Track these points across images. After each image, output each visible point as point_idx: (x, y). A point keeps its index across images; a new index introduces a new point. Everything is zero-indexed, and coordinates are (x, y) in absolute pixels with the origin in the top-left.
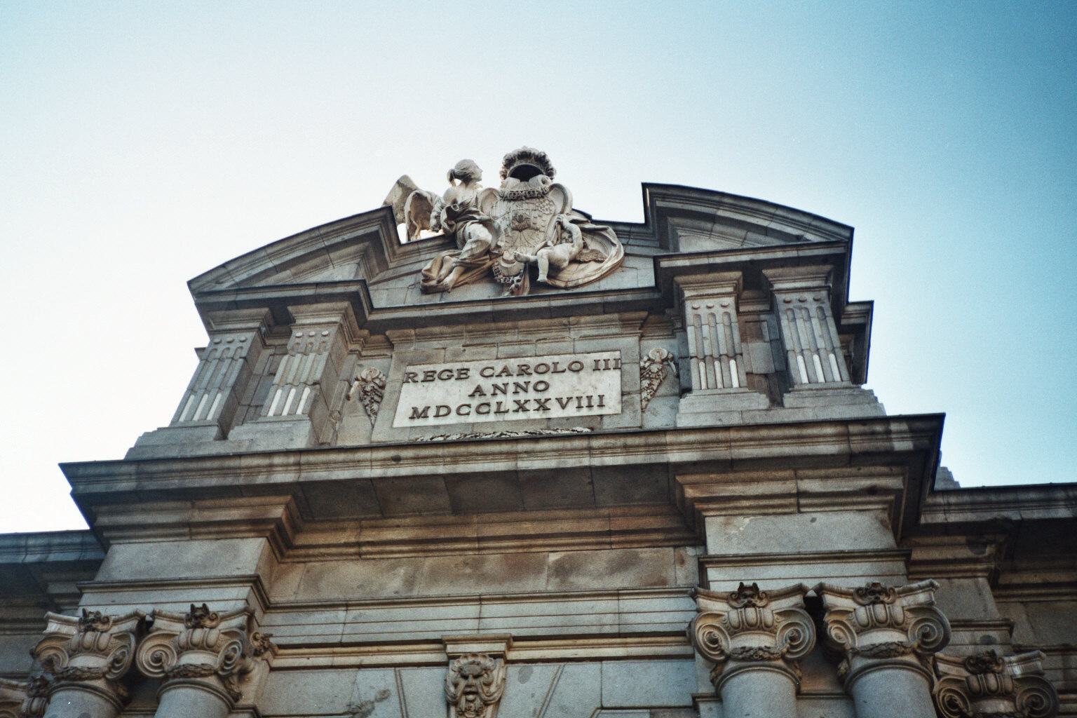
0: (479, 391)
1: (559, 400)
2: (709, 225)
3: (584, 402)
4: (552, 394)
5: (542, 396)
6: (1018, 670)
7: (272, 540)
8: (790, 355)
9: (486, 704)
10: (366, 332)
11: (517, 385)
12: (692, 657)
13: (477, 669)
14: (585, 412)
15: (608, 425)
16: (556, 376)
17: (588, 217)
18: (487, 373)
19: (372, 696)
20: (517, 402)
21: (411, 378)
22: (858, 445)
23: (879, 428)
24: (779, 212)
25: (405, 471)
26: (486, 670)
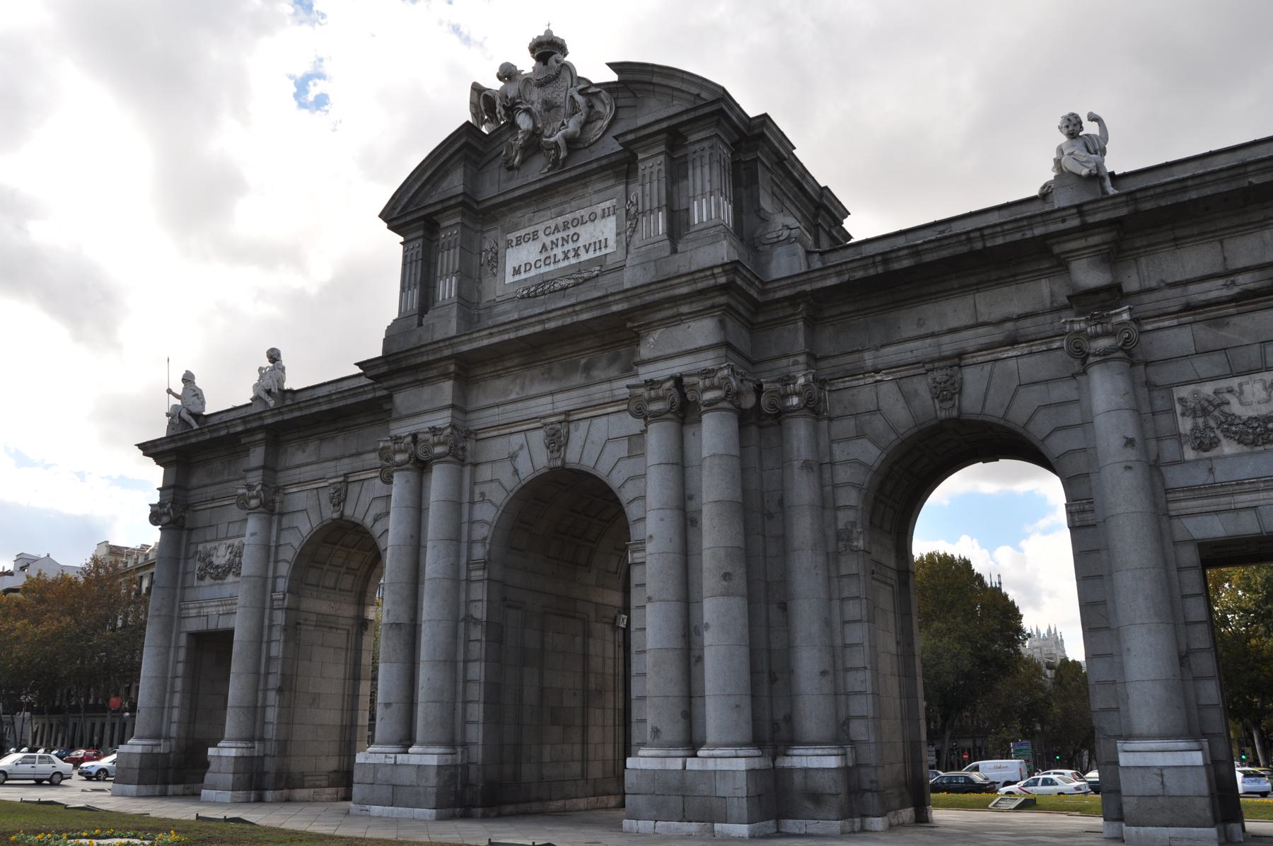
1: (585, 246)
2: (651, 88)
4: (581, 243)
5: (575, 246)
7: (455, 379)
9: (560, 447)
10: (480, 216)
11: (563, 239)
13: (553, 431)
14: (598, 254)
15: (609, 261)
16: (583, 226)
17: (589, 82)
18: (547, 233)
20: (564, 252)
21: (509, 244)
22: (700, 286)
23: (708, 273)
24: (685, 76)
25: (496, 339)
26: (558, 431)
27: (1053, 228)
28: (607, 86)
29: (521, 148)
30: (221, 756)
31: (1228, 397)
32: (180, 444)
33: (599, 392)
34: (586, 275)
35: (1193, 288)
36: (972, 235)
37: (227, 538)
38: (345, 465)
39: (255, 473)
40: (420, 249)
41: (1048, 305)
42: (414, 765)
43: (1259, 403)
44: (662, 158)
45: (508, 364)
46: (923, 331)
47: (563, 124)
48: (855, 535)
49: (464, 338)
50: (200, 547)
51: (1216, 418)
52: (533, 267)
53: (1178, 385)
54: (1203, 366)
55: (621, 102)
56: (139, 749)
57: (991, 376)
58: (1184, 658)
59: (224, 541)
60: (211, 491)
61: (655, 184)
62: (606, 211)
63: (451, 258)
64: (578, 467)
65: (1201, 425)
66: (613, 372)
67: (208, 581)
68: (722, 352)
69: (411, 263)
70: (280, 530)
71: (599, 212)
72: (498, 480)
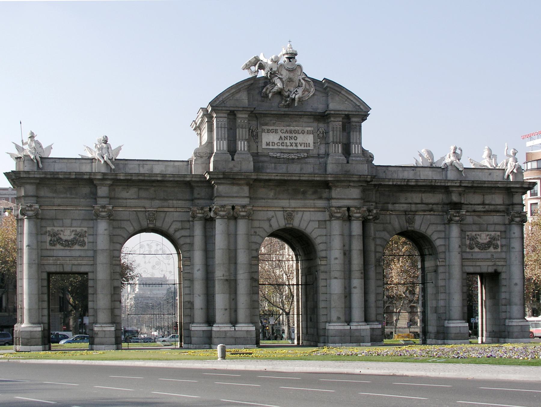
0: (281, 136)
1: (300, 143)
2: (339, 93)
4: (298, 141)
5: (296, 142)
8: (351, 144)
11: (290, 137)
12: (325, 211)
13: (290, 214)
14: (305, 148)
17: (307, 76)
18: (282, 131)
19: (271, 216)
20: (290, 143)
21: (263, 131)
22: (361, 179)
27: (453, 184)
30: (104, 331)
31: (478, 236)
33: (310, 202)
34: (303, 156)
36: (433, 181)
37: (71, 227)
38: (157, 203)
39: (104, 200)
40: (226, 123)
41: (441, 201)
42: (245, 331)
44: (341, 123)
45: (270, 184)
46: (407, 202)
47: (296, 91)
49: (265, 174)
51: (475, 242)
52: (276, 145)
53: (467, 231)
54: (474, 227)
55: (317, 88)
56: (39, 329)
59: (68, 228)
60: (57, 201)
63: (244, 132)
65: (472, 243)
66: (313, 197)
67: (59, 246)
68: (362, 201)
70: (113, 228)
71: (306, 131)
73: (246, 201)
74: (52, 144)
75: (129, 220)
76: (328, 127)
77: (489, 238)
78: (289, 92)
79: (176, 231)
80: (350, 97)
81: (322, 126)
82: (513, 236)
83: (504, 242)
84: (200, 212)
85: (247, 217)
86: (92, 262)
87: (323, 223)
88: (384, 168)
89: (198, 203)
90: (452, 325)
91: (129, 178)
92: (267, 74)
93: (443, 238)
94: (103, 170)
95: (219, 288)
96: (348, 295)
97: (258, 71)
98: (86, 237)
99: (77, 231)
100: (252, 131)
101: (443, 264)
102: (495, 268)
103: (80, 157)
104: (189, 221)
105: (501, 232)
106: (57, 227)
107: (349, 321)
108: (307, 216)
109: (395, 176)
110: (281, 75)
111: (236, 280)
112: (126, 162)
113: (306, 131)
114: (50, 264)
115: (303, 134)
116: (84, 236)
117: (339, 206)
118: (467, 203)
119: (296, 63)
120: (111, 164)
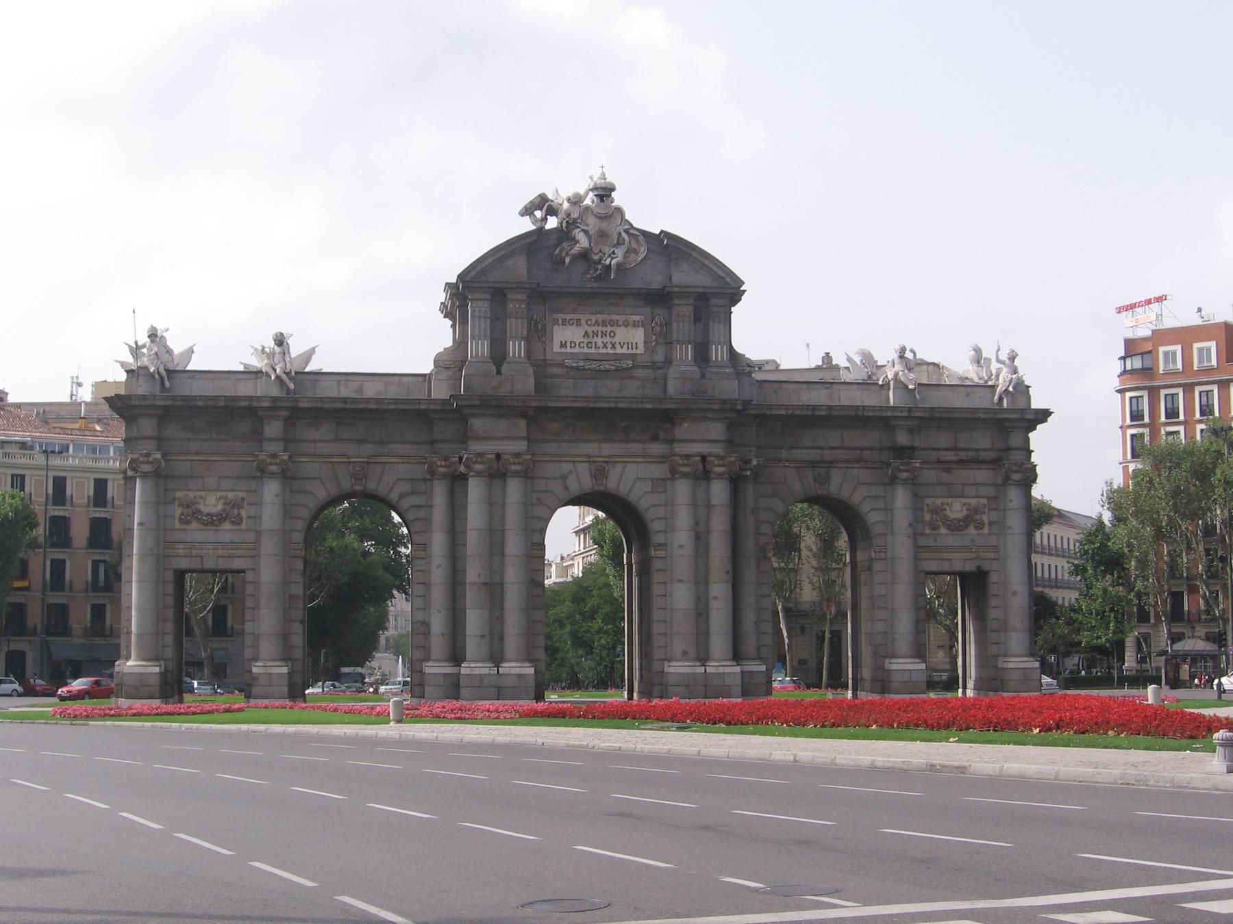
1: (620, 343)
3: (630, 345)
4: (617, 339)
5: (613, 340)
6: (755, 463)
12: (664, 462)
14: (630, 351)
17: (631, 225)
18: (588, 323)
20: (603, 342)
21: (556, 322)
24: (718, 263)
27: (896, 414)
28: (645, 234)
29: (575, 254)
30: (270, 674)
32: (180, 403)
33: (635, 447)
34: (624, 366)
35: (941, 453)
37: (218, 490)
38: (369, 448)
40: (489, 310)
43: (958, 512)
44: (691, 308)
47: (614, 253)
48: (768, 550)
50: (179, 494)
56: (157, 670)
57: (845, 475)
58: (918, 621)
61: (687, 324)
62: (637, 322)
64: (614, 492)
67: (194, 525)
69: (480, 317)
70: (291, 491)
71: (631, 322)
72: (550, 491)
73: (521, 446)
74: (194, 345)
75: (320, 478)
76: (670, 314)
77: (967, 510)
78: (600, 254)
79: (401, 496)
80: (707, 263)
81: (661, 314)
82: (1010, 505)
83: (994, 516)
84: (443, 463)
85: (523, 474)
86: (251, 553)
87: (659, 484)
88: (775, 385)
89: (440, 449)
90: (895, 667)
91: (319, 405)
92: (561, 224)
93: (881, 509)
94: (275, 391)
95: (472, 597)
96: (701, 611)
97: (546, 219)
98: (243, 508)
99: (227, 498)
100: (537, 323)
101: (883, 555)
102: (978, 563)
103: (241, 368)
104: (425, 480)
105: (988, 498)
106: (192, 490)
107: (703, 659)
108: (632, 470)
109: (794, 400)
110: (587, 225)
111: (503, 584)
112: (317, 377)
113: (631, 322)
114: (179, 556)
115: (626, 326)
116: (240, 507)
117: (687, 453)
118: (925, 447)
119: (613, 204)
120: (288, 381)
